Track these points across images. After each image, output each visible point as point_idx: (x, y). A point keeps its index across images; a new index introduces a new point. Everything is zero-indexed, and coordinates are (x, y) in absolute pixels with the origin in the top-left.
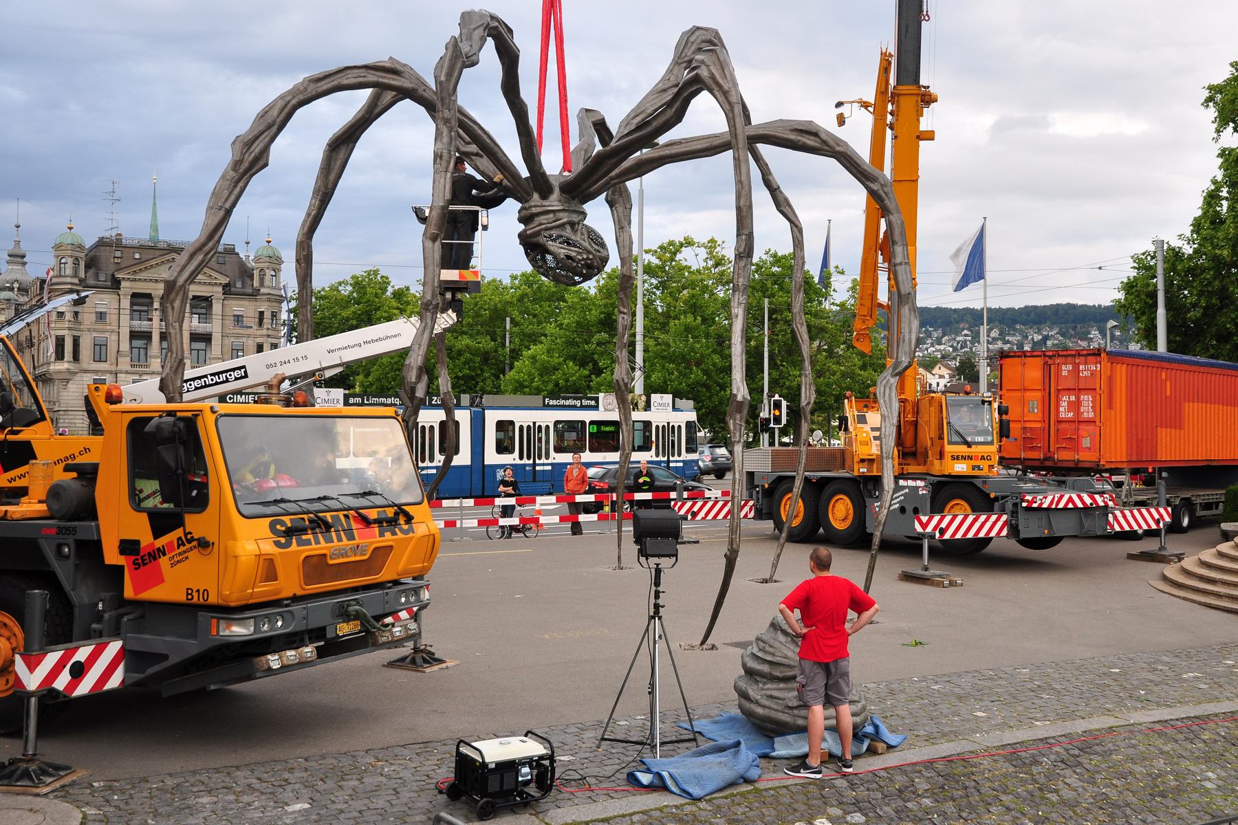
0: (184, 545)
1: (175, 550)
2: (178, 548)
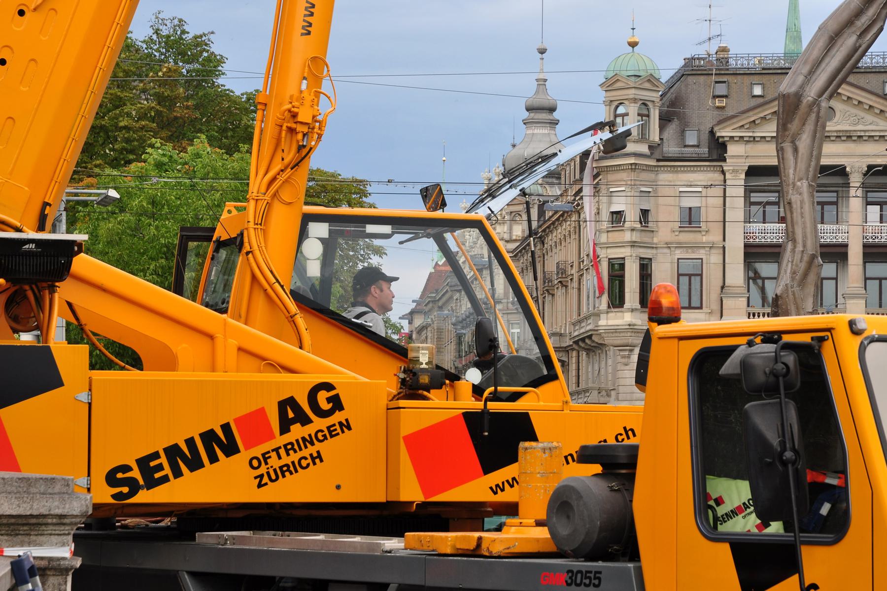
0: (305, 421)
1: (272, 437)
2: (284, 429)
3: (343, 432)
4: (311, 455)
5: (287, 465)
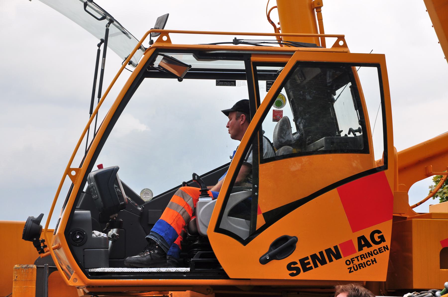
0: (369, 246)
1: (355, 252)
2: (360, 249)
3: (385, 251)
4: (372, 260)
5: (361, 264)
